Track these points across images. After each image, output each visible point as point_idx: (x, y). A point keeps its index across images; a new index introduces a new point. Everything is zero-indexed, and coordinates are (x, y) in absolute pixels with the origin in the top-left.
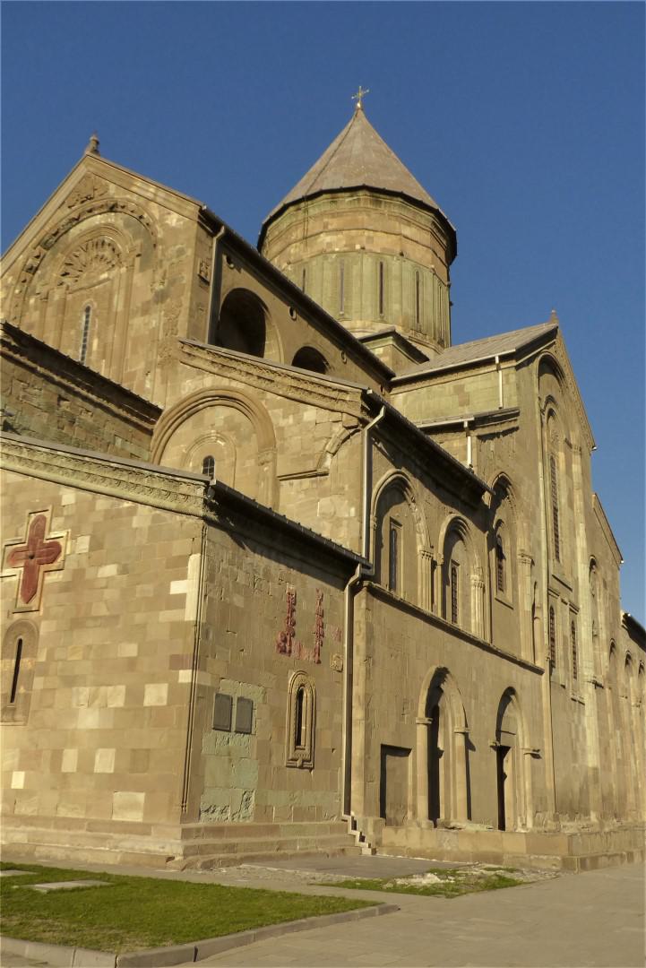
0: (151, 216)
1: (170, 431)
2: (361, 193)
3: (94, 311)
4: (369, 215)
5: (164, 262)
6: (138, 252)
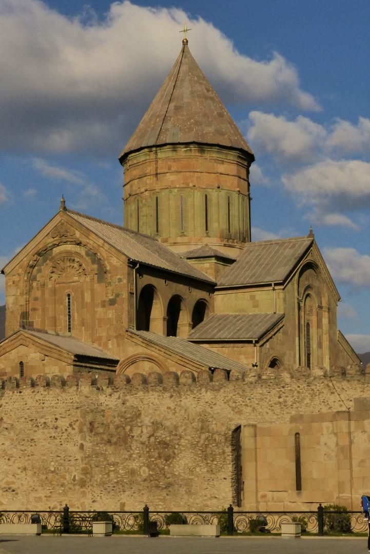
1: (124, 370)
2: (192, 146)
3: (73, 297)
4: (197, 161)
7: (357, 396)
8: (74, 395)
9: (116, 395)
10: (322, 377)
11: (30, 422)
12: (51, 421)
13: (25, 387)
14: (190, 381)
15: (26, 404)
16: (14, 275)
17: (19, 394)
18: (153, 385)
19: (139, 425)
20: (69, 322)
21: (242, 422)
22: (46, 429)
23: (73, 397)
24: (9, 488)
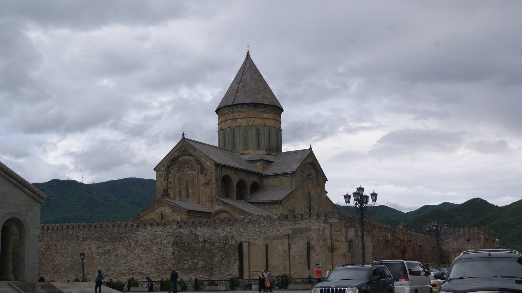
0: (203, 162)
5: (207, 174)
6: (200, 169)
7: (292, 228)
8: (170, 229)
9: (188, 229)
10: (277, 219)
11: (150, 242)
12: (159, 241)
13: (148, 226)
14: (220, 222)
15: (148, 234)
16: (160, 171)
17: (145, 229)
18: (204, 224)
19: (198, 242)
20: (187, 194)
21: (243, 240)
23: (169, 230)
24: (141, 272)
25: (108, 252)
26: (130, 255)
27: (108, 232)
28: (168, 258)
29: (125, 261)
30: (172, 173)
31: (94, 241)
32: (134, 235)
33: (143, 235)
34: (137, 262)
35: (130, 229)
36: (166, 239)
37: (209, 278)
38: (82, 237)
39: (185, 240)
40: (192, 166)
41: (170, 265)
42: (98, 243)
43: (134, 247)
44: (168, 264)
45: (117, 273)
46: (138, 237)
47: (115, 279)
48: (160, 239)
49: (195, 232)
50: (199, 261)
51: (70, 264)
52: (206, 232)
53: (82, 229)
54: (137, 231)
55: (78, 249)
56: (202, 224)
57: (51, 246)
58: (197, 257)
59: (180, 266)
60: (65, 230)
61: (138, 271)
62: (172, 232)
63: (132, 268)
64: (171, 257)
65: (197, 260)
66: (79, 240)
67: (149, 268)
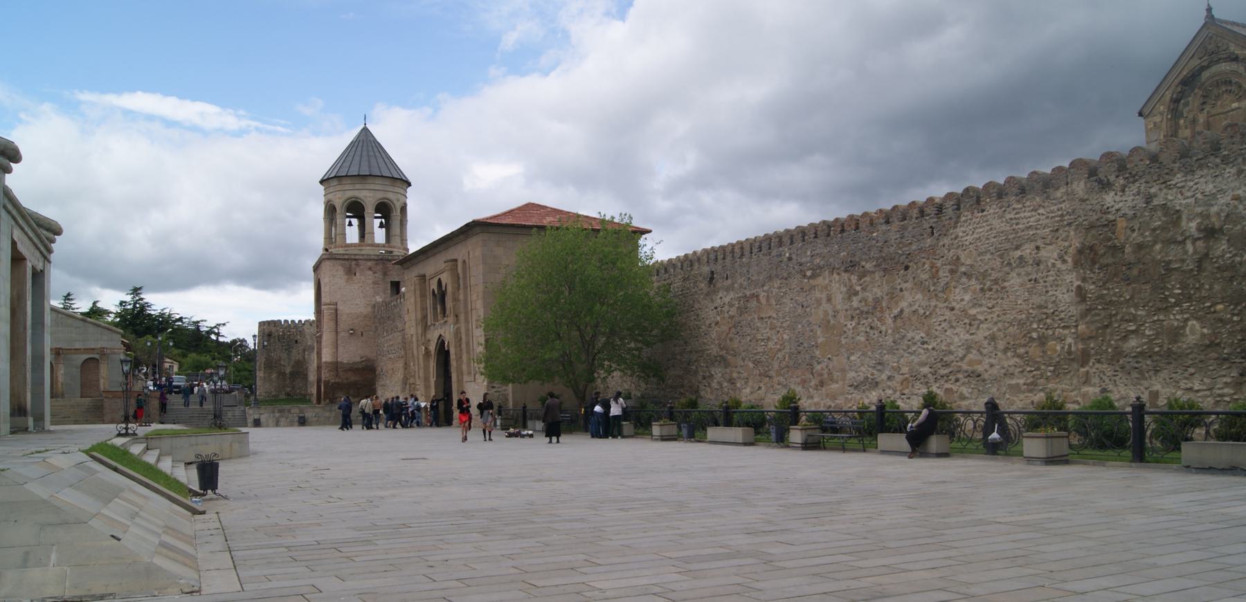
8: (1064, 201)
9: (1134, 188)
12: (1030, 254)
13: (988, 200)
15: (991, 229)
16: (1154, 116)
17: (980, 214)
18: (1200, 157)
19: (1180, 238)
22: (1023, 267)
23: (1063, 205)
24: (972, 373)
25: (875, 308)
26: (937, 310)
27: (874, 242)
28: (1062, 315)
29: (923, 335)
30: (1185, 115)
31: (838, 274)
32: (946, 241)
33: (975, 236)
34: (960, 336)
35: (936, 220)
36: (1050, 244)
37: (1234, 394)
38: (811, 267)
39: (1122, 238)
40: (1240, 86)
41: (1069, 340)
42: (849, 279)
43: (947, 283)
44: (1065, 336)
45: (903, 374)
46: (959, 246)
47: (898, 393)
48: (1033, 245)
49: (1166, 199)
50: (1187, 320)
51: (791, 349)
52: (1214, 191)
53: (811, 242)
54: (955, 227)
55: (805, 304)
56: (1195, 158)
57: (748, 301)
58: (1176, 304)
59: (1110, 346)
60: (774, 252)
61: (965, 367)
62: (1074, 211)
63: (945, 355)
64: (1075, 310)
65: (1177, 317)
66: (805, 276)
67: (999, 354)
